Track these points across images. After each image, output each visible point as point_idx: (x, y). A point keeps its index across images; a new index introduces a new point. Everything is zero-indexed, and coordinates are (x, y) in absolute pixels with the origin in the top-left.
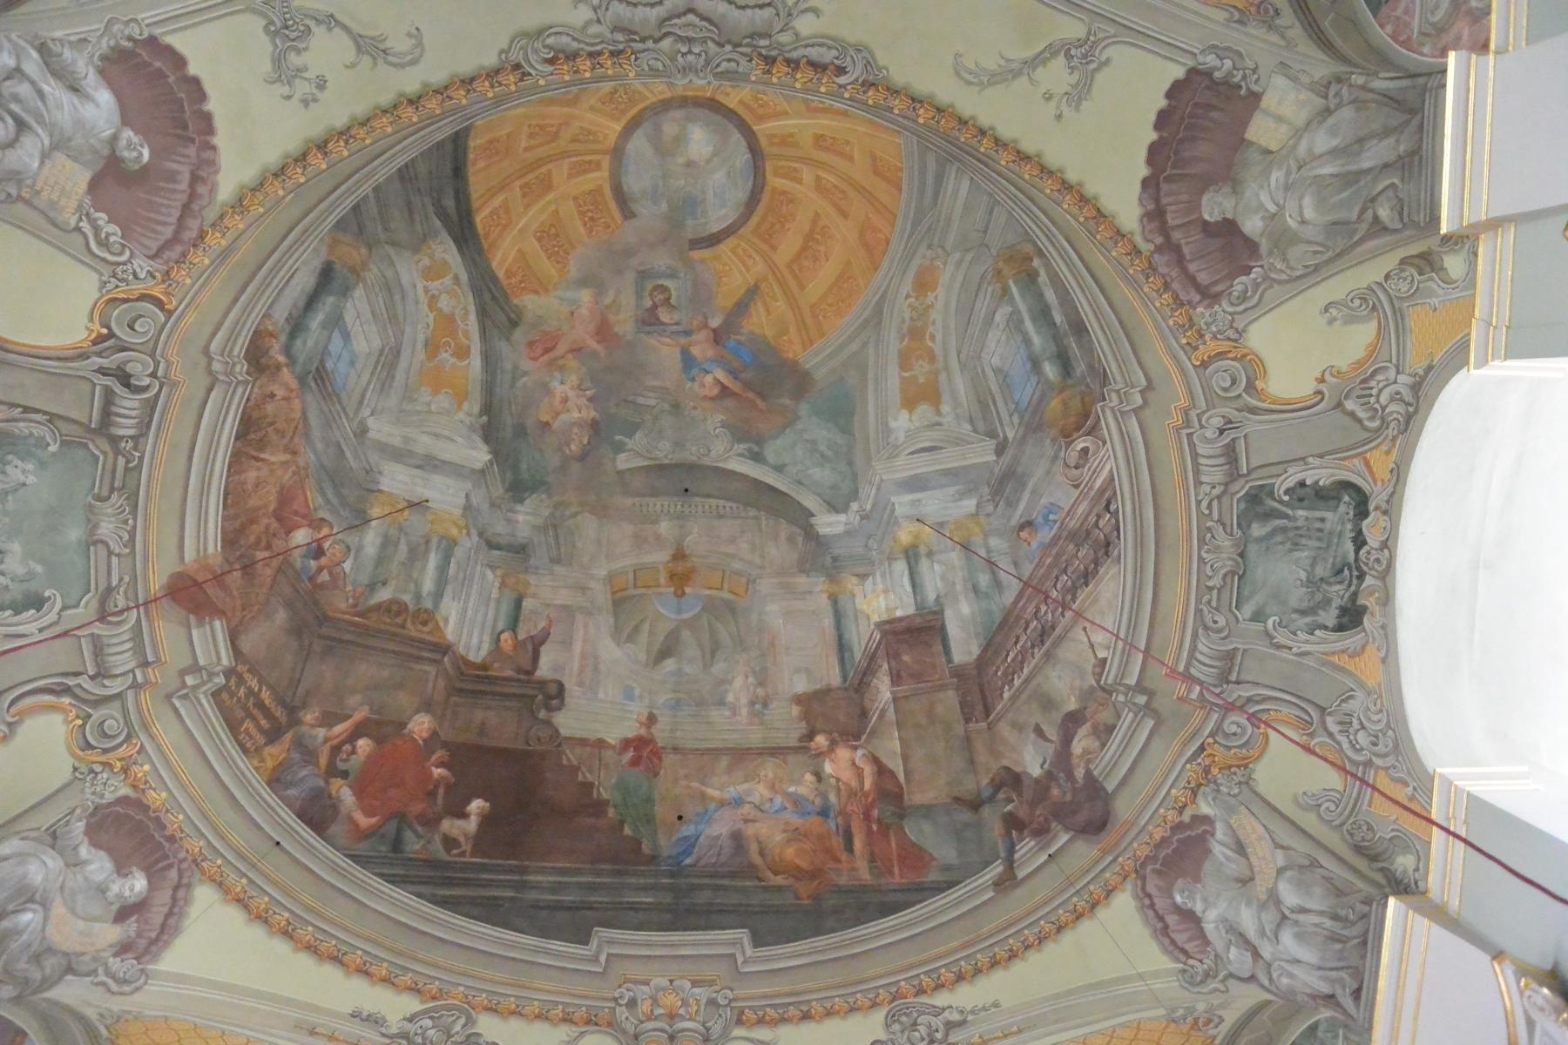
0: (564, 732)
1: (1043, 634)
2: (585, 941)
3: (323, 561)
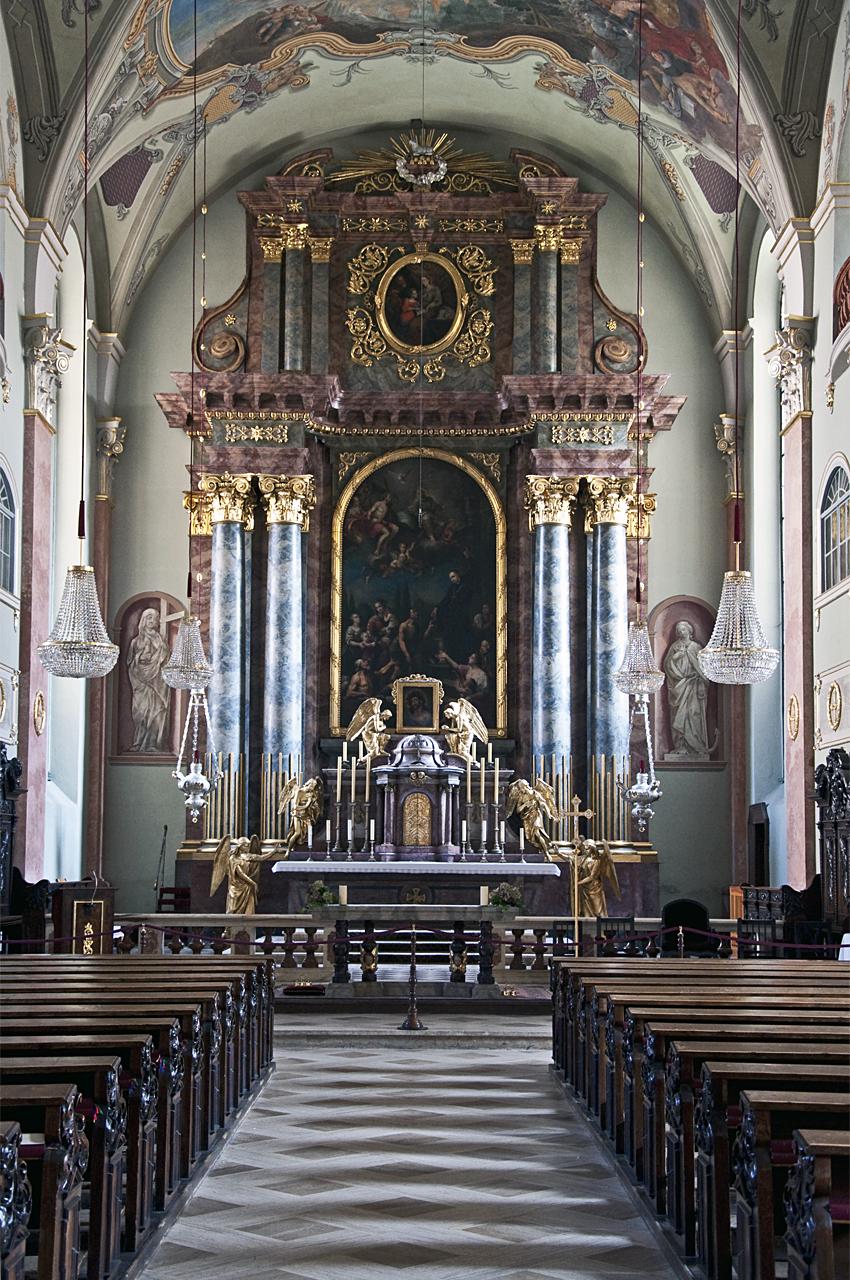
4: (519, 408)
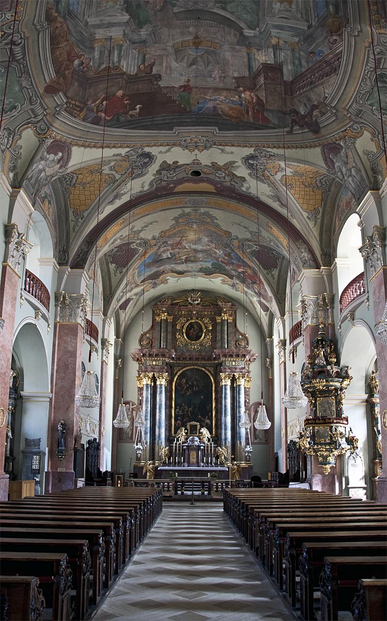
0: (162, 86)
1: (311, 83)
2: (172, 130)
3: (84, 65)
4: (218, 357)
